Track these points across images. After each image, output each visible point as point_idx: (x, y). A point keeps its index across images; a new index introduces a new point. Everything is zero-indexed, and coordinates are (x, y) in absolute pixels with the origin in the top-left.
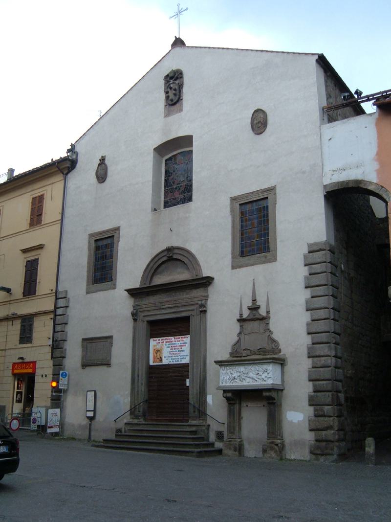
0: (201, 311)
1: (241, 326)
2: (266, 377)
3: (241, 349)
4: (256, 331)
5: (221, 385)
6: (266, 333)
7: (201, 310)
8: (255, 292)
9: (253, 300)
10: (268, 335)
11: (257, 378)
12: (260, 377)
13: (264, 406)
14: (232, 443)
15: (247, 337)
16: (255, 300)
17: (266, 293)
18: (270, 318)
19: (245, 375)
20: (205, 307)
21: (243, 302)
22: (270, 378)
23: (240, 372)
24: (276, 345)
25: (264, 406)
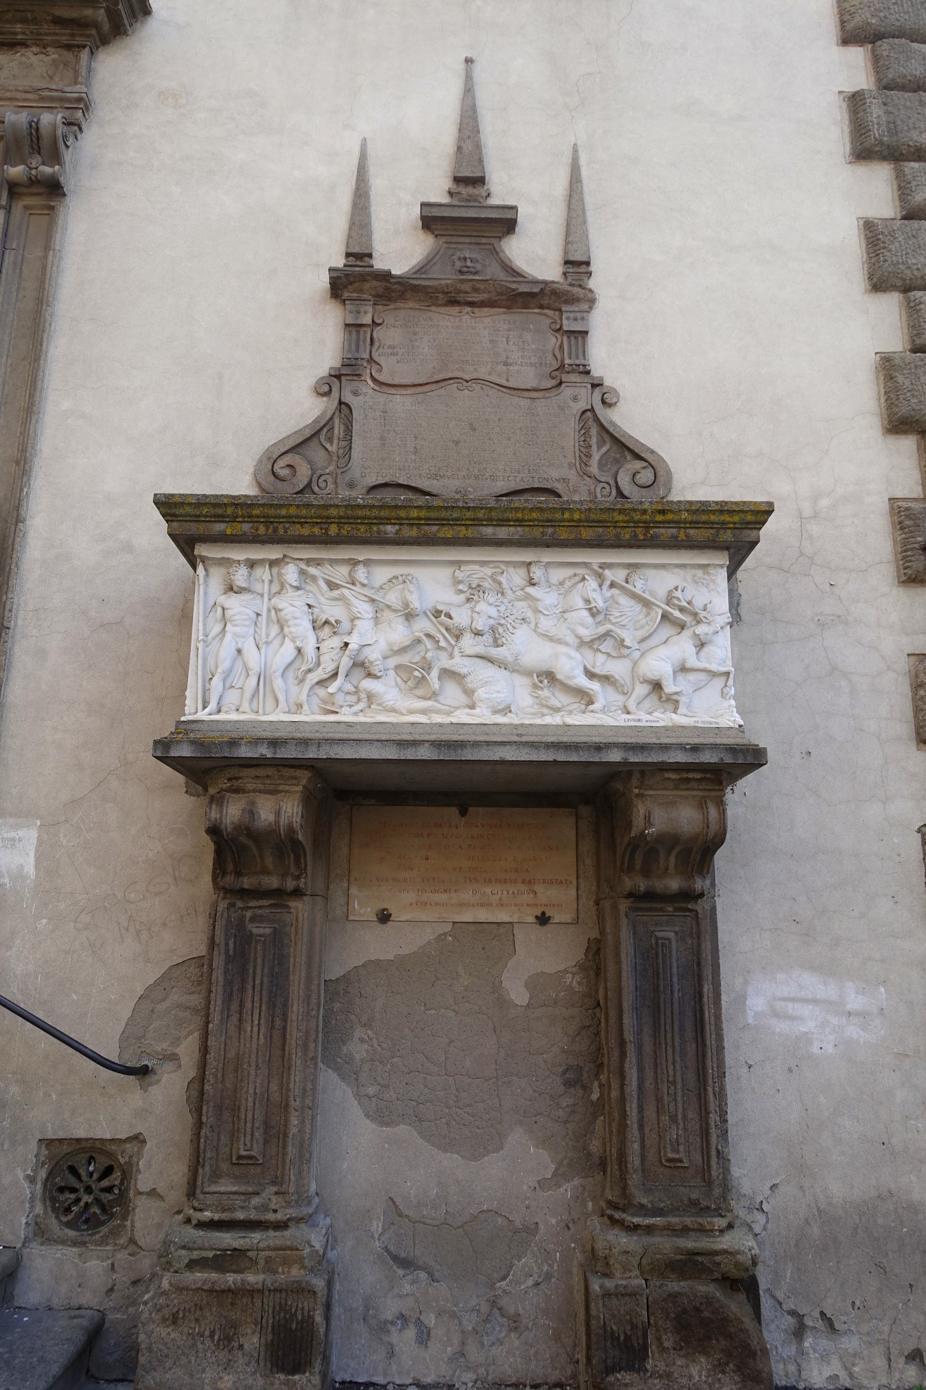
0: (14, 189)
1: (352, 328)
2: (683, 669)
3: (351, 485)
4: (483, 372)
5: (193, 711)
6: (567, 392)
7: (16, 171)
8: (477, 131)
9: (457, 180)
10: (582, 405)
11: (591, 675)
12: (618, 669)
13: (543, 920)
14: (253, 1278)
15: (401, 403)
16: (480, 181)
17: (567, 159)
18: (592, 301)
19: (468, 643)
20: (55, 157)
21: (378, 184)
22: (713, 674)
23: (409, 616)
24: (646, 476)
25: (543, 920)
